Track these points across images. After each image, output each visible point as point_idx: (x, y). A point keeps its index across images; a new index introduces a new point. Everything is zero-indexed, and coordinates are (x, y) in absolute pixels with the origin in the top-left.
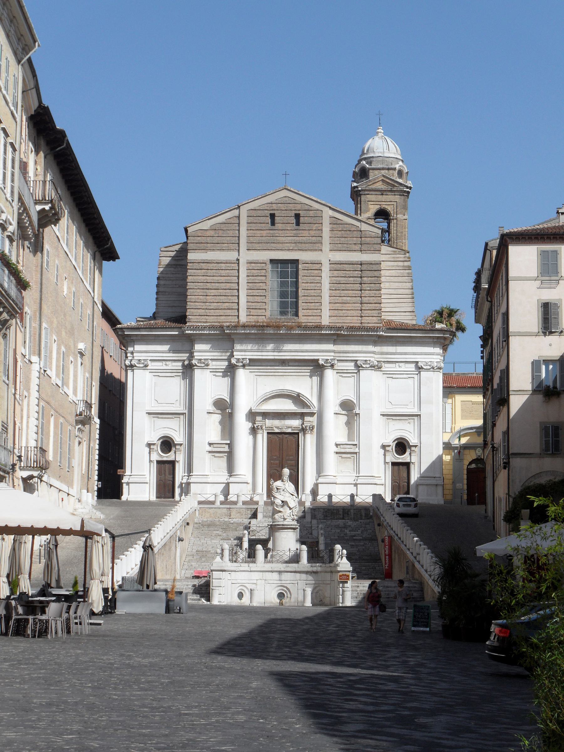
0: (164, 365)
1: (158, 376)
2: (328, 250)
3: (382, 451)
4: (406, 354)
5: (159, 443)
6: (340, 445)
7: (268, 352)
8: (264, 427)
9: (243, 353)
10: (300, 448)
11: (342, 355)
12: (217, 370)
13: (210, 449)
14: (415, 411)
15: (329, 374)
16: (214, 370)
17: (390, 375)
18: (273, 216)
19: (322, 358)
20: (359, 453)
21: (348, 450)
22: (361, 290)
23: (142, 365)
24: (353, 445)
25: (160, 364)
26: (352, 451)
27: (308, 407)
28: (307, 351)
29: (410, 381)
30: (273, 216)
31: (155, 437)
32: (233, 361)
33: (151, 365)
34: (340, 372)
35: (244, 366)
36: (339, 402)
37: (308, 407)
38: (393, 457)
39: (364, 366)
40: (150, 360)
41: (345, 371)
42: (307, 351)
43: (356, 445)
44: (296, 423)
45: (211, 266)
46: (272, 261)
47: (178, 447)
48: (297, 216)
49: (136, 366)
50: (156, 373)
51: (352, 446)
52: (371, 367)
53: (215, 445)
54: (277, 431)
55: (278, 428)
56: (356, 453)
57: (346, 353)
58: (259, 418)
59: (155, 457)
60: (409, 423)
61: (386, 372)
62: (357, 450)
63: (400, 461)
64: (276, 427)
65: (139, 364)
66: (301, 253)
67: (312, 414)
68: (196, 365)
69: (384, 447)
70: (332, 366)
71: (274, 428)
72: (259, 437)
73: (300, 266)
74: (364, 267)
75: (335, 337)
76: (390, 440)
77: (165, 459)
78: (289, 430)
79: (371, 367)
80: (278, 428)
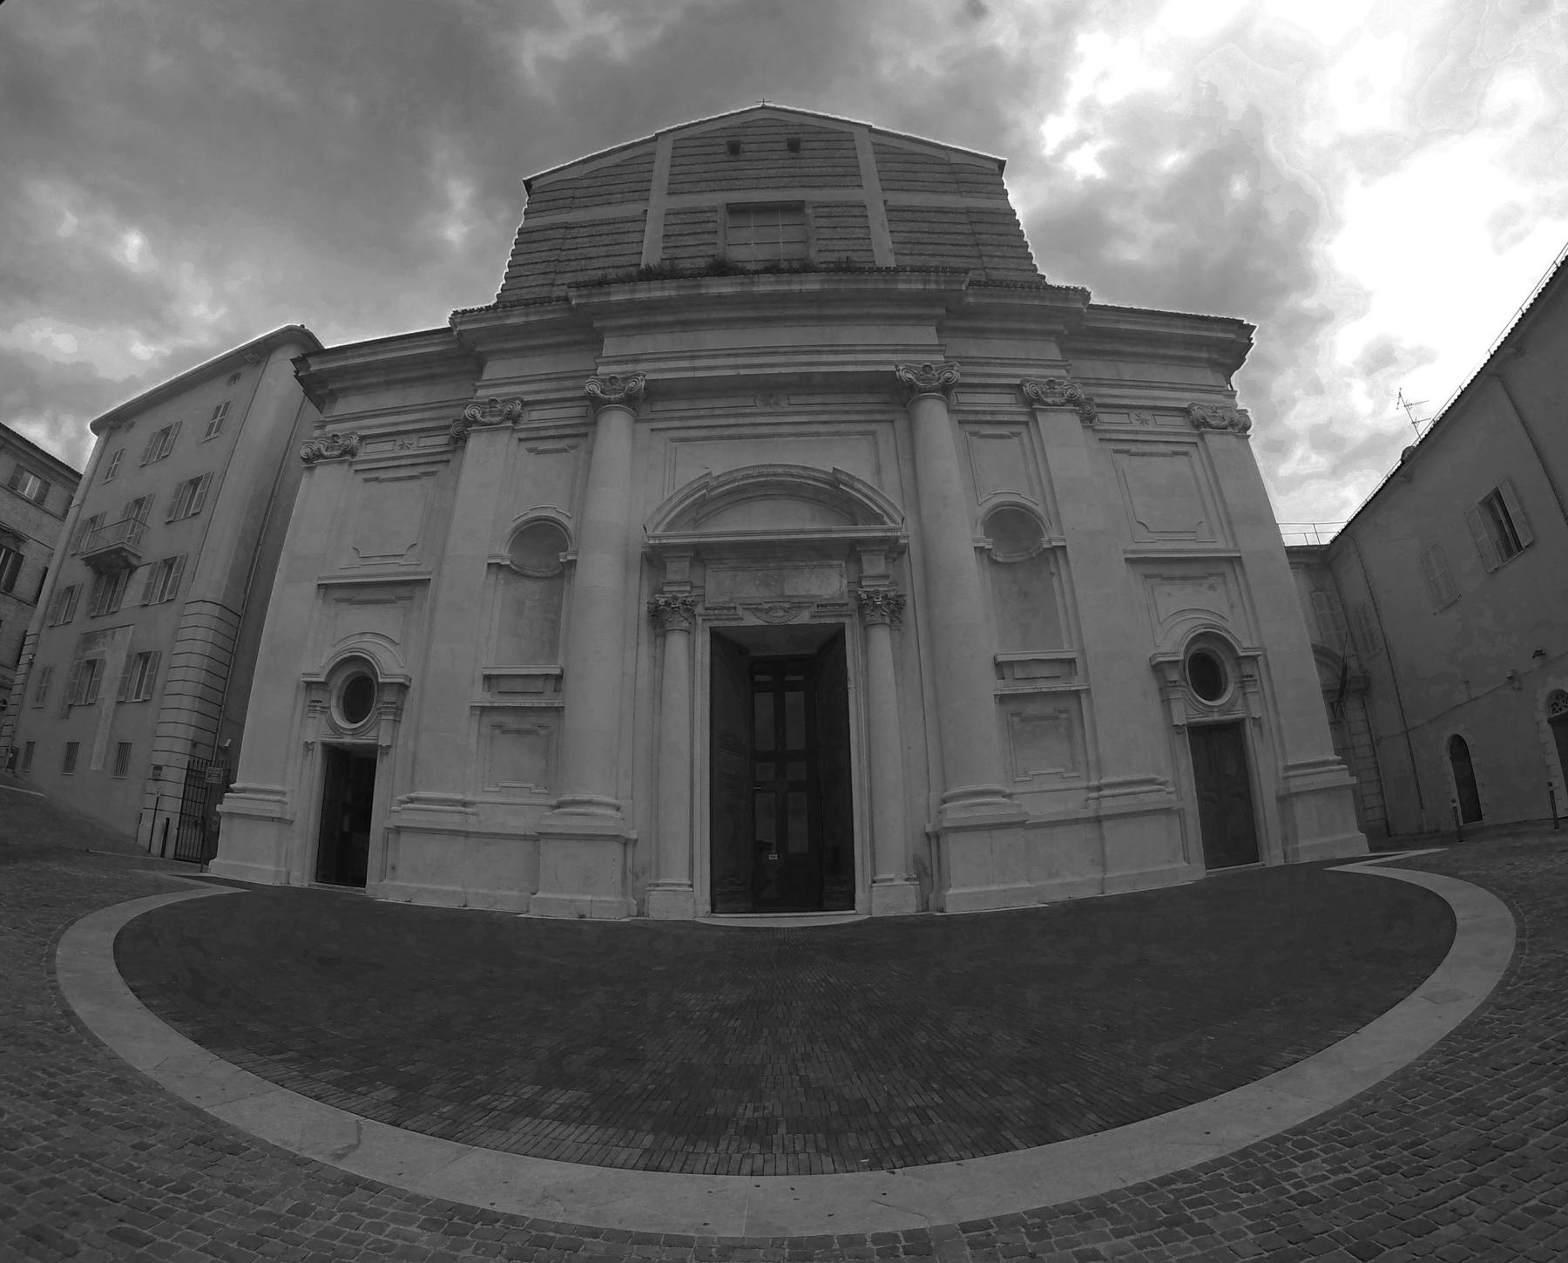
0: (397, 448)
1: (377, 479)
2: (877, 185)
3: (1152, 686)
4: (1150, 386)
5: (340, 680)
6: (1011, 664)
7: (720, 351)
8: (699, 610)
9: (630, 367)
10: (851, 685)
11: (967, 369)
12: (543, 433)
13: (482, 697)
14: (1220, 545)
15: (934, 416)
16: (534, 434)
17: (1123, 446)
18: (734, 149)
19: (903, 367)
20: (1088, 691)
21: (1044, 686)
22: (980, 257)
23: (336, 453)
24: (1061, 661)
25: (388, 446)
26: (1059, 686)
27: (877, 519)
28: (851, 349)
29: (1181, 464)
30: (734, 149)
31: (317, 663)
32: (593, 387)
33: (367, 452)
34: (967, 421)
35: (631, 402)
36: (982, 511)
37: (877, 519)
38: (1188, 709)
39: (1049, 400)
40: (362, 438)
41: (989, 418)
42: (851, 349)
43: (1071, 661)
44: (827, 585)
45: (574, 232)
46: (735, 210)
47: (388, 697)
48: (794, 146)
49: (321, 456)
50: (373, 474)
51: (1056, 670)
52: (1068, 401)
53: (504, 686)
54: (751, 620)
55: (755, 609)
56: (1077, 693)
57: (979, 364)
58: (677, 570)
59: (317, 732)
60: (1211, 587)
61: (1108, 436)
62: (1077, 684)
63: (1216, 717)
64: (748, 607)
65: (332, 449)
66: (808, 191)
67: (894, 549)
68: (476, 421)
69: (1158, 668)
70: (946, 389)
71: (740, 612)
72: (677, 644)
73: (809, 211)
74: (974, 218)
75: (941, 311)
76: (1173, 643)
77: (348, 740)
78: (804, 618)
79: (1068, 401)
80: (755, 609)
